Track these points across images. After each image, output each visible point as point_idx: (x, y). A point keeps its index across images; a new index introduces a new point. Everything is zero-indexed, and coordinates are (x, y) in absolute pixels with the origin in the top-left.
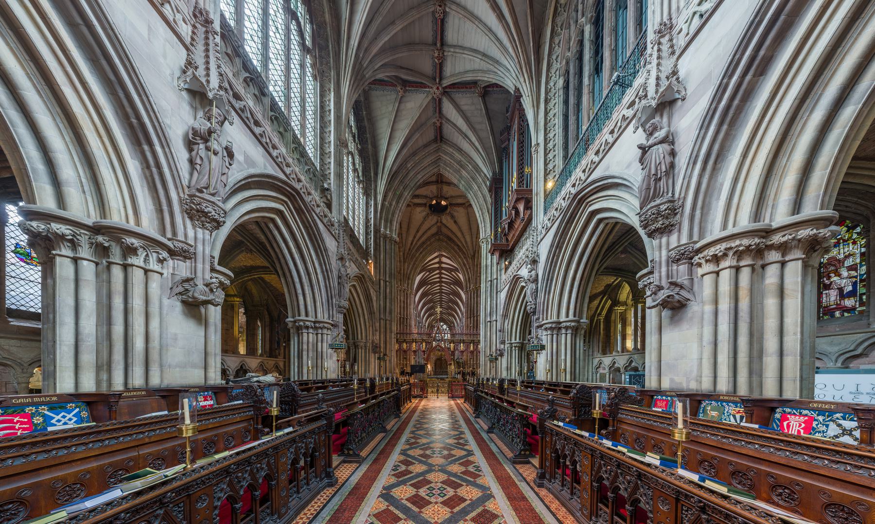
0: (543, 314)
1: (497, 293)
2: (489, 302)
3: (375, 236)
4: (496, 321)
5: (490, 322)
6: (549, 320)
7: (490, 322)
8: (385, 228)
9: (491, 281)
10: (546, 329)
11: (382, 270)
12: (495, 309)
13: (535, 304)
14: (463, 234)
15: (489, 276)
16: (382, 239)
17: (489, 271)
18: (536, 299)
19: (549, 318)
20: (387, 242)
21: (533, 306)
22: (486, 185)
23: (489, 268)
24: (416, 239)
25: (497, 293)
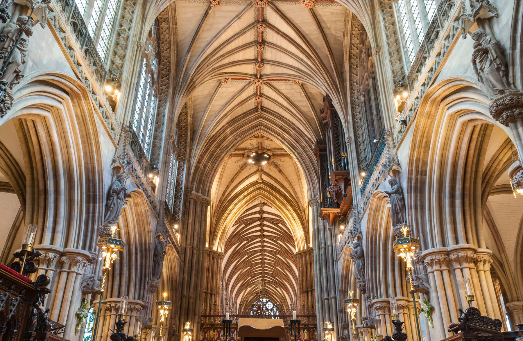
0: (373, 292)
1: (333, 263)
2: (324, 274)
3: (185, 200)
4: (335, 298)
5: (328, 299)
6: (379, 299)
7: (328, 299)
8: (197, 191)
9: (325, 249)
10: (377, 309)
11: (189, 236)
12: (332, 283)
13: (364, 282)
14: (290, 184)
15: (322, 241)
16: (192, 202)
17: (322, 236)
18: (364, 276)
19: (379, 296)
20: (198, 205)
21: (362, 284)
22: (311, 148)
23: (322, 233)
24: (230, 189)
25: (333, 263)
